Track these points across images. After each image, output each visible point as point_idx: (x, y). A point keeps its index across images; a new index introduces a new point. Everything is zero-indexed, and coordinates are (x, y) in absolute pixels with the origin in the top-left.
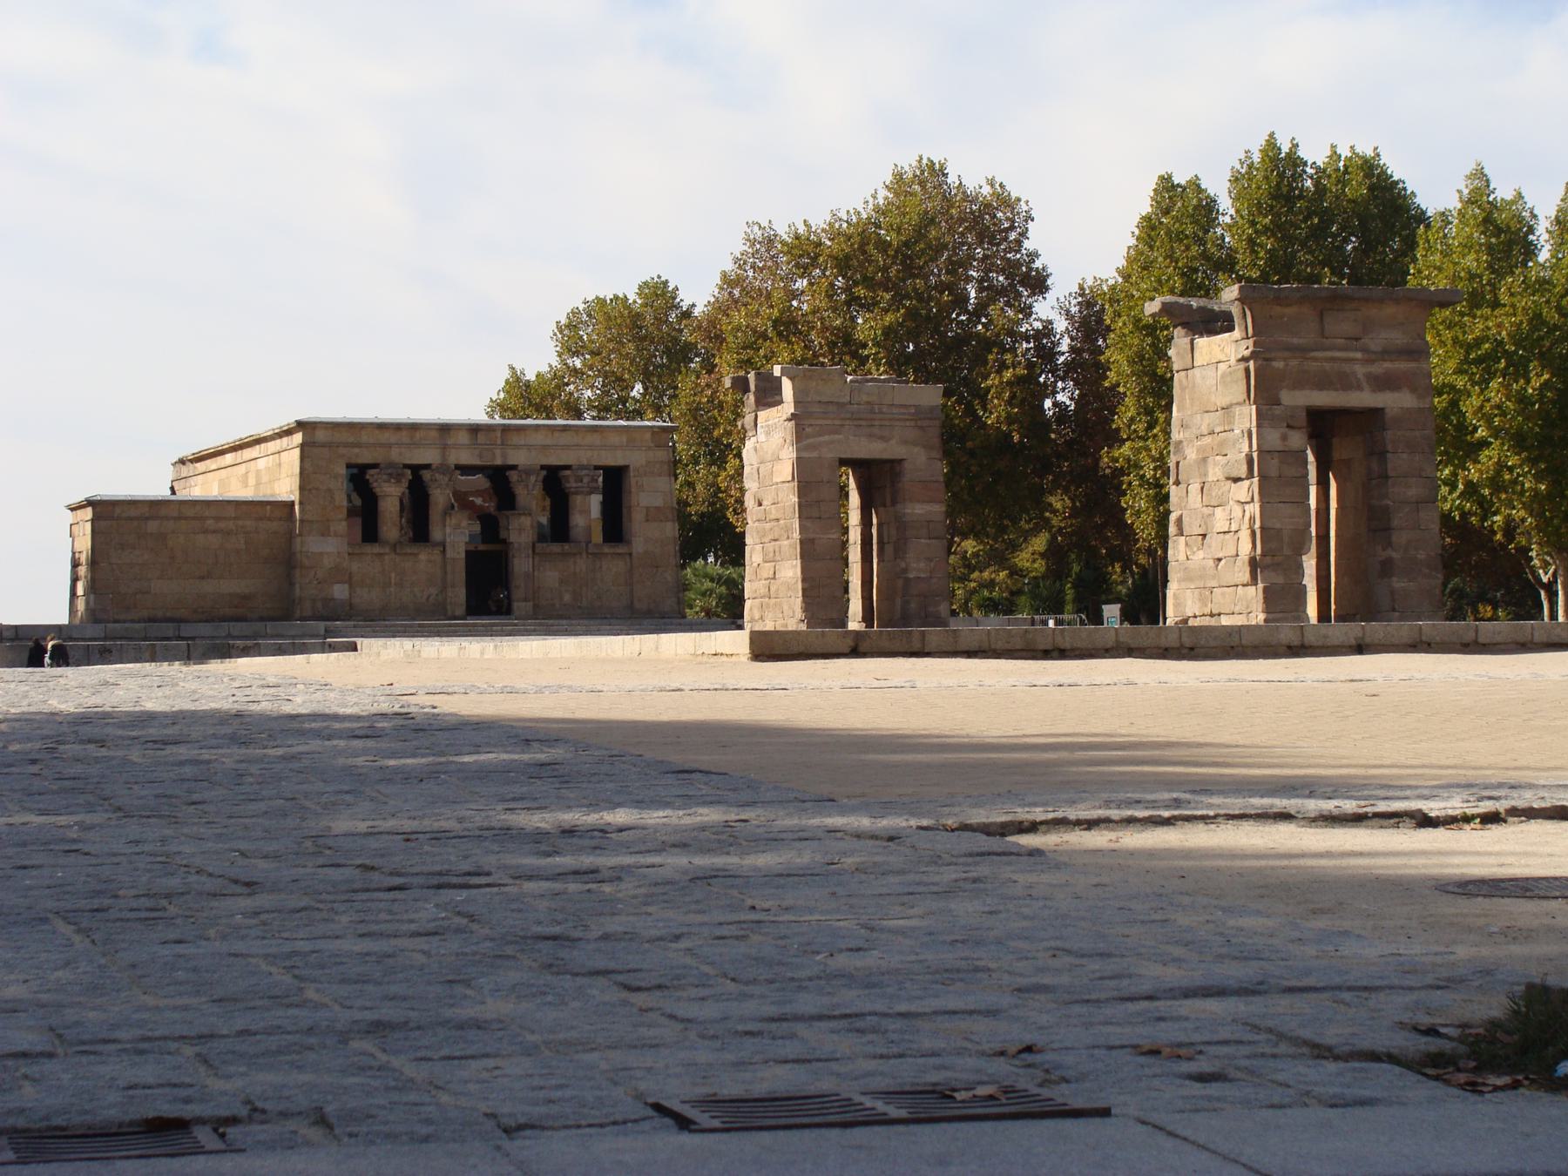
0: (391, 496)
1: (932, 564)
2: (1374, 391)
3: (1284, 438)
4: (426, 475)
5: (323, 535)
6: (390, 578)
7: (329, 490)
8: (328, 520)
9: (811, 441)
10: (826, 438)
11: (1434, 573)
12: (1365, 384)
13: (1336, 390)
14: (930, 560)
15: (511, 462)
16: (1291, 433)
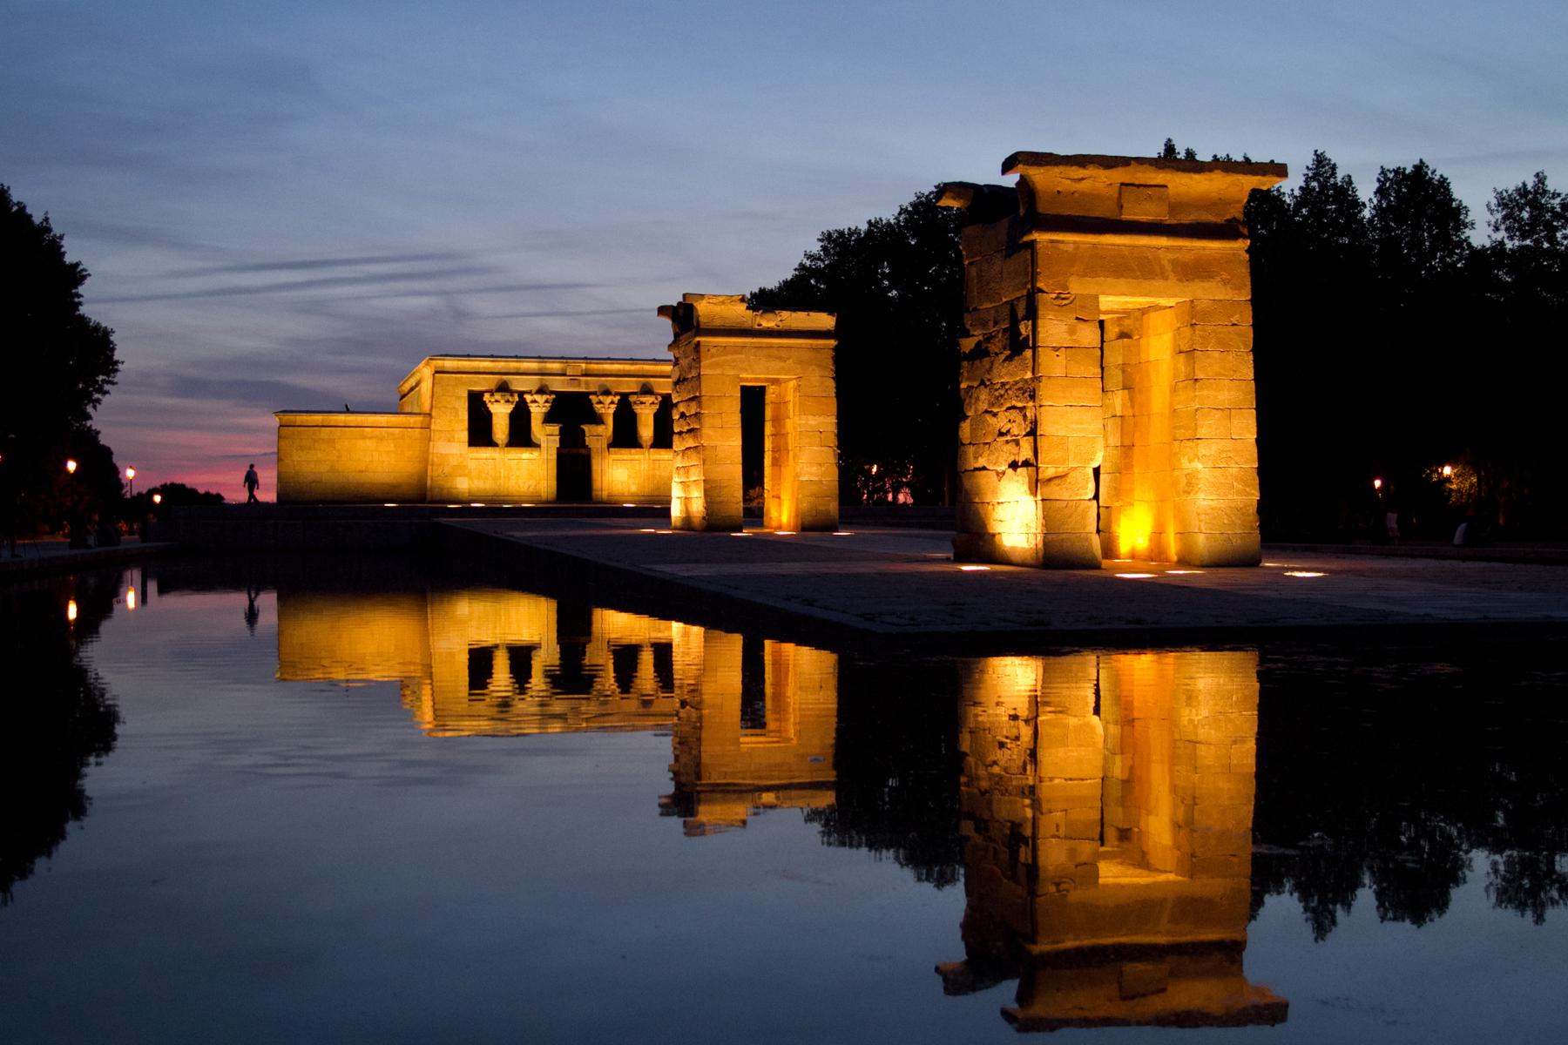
0: (501, 412)
1: (823, 469)
2: (1180, 280)
3: (1072, 331)
4: (528, 398)
5: (449, 441)
6: (500, 472)
7: (454, 408)
8: (453, 430)
9: (713, 360)
10: (729, 357)
11: (1248, 489)
12: (1172, 275)
13: (1136, 278)
14: (820, 464)
15: (592, 390)
16: (1081, 325)
